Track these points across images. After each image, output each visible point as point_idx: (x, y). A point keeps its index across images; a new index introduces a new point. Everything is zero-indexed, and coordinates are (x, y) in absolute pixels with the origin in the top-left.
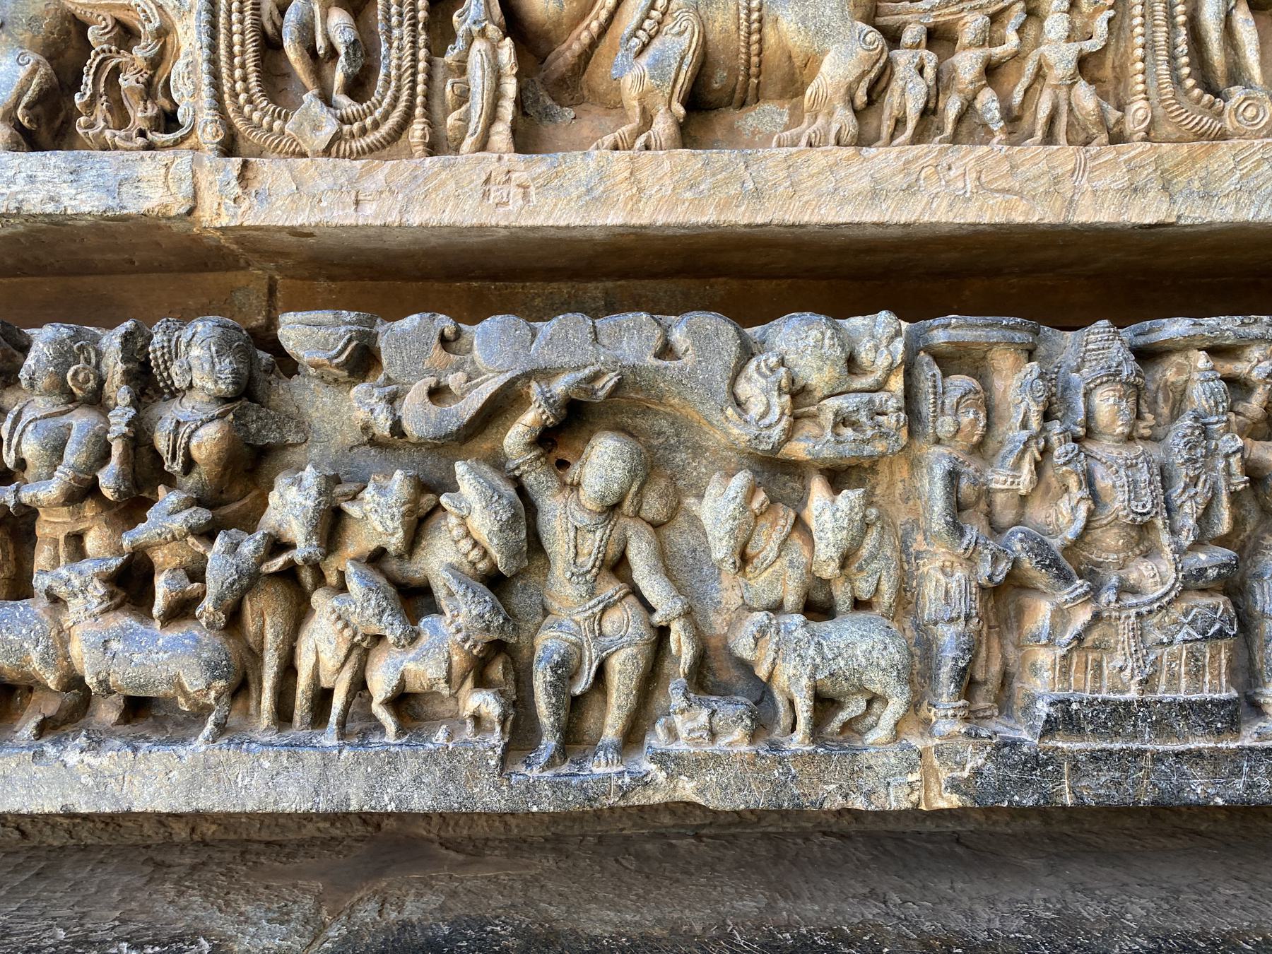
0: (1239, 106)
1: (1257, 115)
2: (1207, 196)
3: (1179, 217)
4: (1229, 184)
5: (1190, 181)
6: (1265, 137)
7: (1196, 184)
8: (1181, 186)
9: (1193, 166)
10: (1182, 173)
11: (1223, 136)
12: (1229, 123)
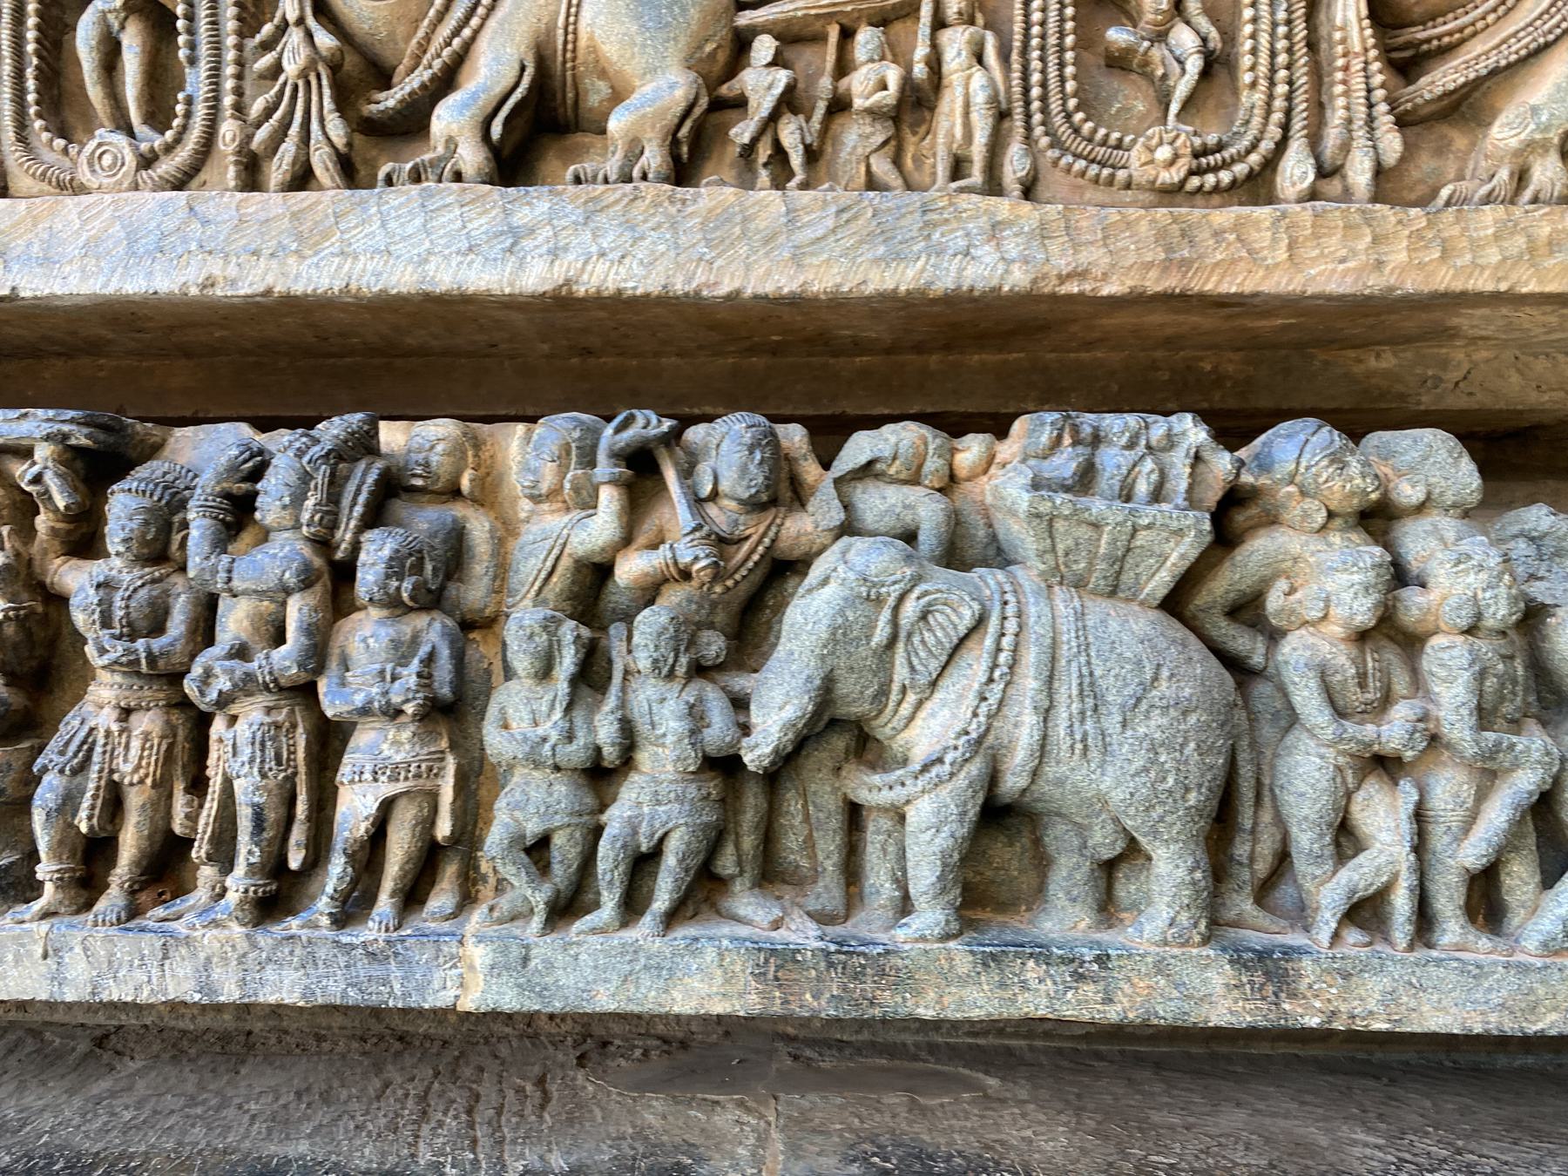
0: (93, 152)
1: (114, 164)
2: (46, 261)
3: (14, 289)
4: (73, 250)
5: (29, 244)
6: (129, 190)
7: (36, 248)
8: (20, 250)
9: (35, 225)
10: (21, 236)
11: (77, 189)
12: (84, 175)
